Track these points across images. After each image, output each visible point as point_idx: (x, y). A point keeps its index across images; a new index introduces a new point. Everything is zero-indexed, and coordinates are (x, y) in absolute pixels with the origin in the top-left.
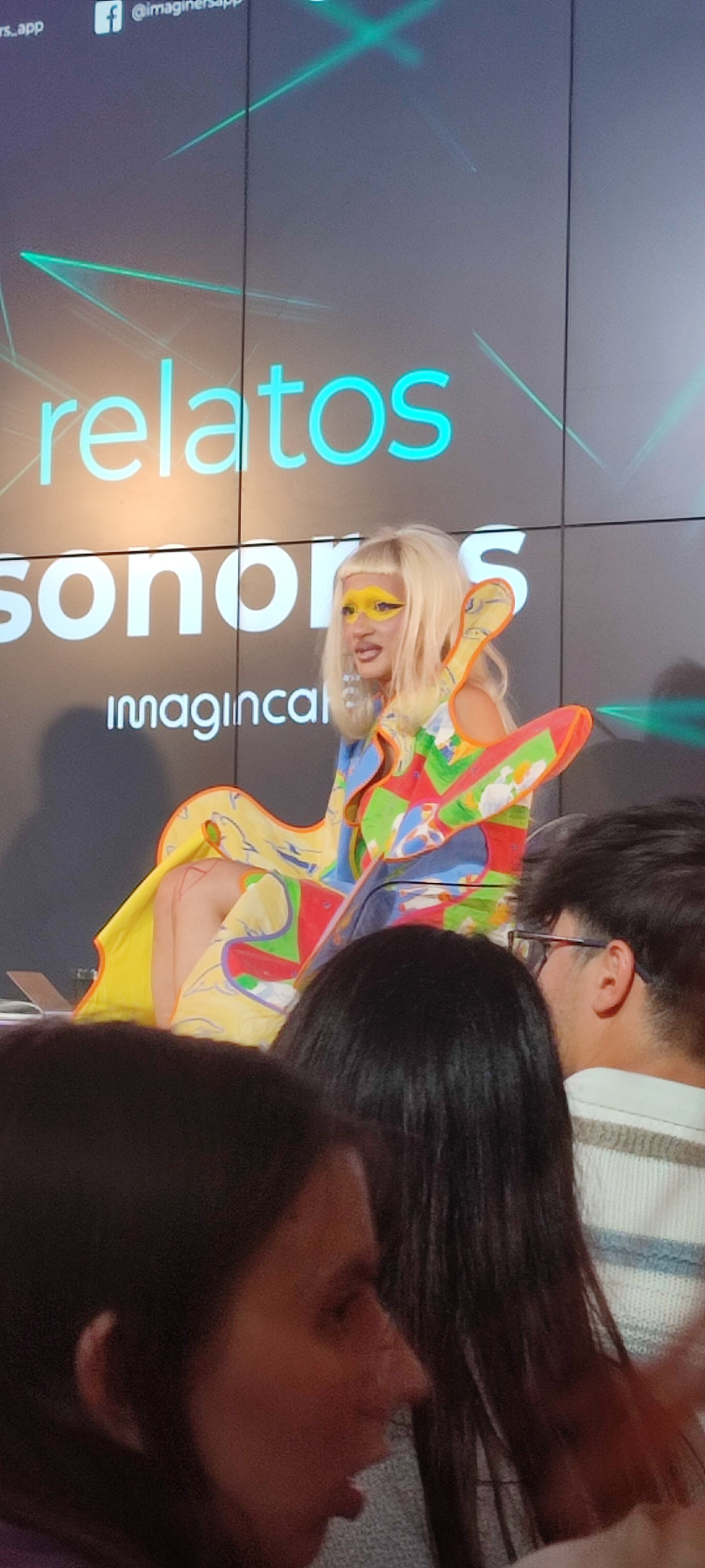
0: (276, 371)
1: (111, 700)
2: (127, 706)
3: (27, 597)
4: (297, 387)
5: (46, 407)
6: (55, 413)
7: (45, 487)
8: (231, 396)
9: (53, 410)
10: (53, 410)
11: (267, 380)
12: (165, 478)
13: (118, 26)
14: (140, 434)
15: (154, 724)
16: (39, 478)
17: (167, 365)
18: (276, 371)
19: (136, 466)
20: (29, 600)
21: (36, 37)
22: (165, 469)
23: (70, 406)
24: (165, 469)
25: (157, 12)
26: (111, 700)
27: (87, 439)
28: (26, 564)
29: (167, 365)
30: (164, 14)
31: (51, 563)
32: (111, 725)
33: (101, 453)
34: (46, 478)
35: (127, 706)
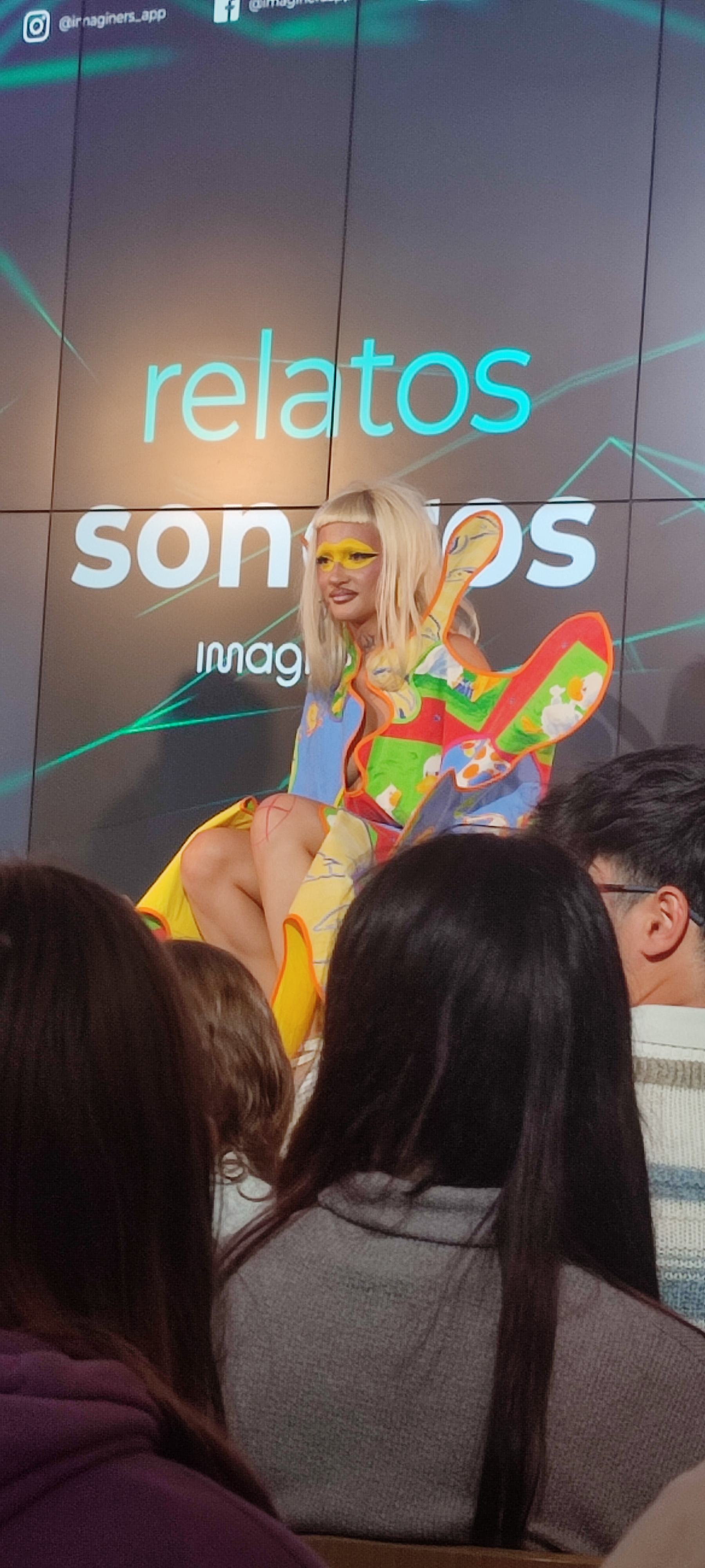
0: (369, 344)
1: (201, 646)
2: (215, 652)
4: (388, 360)
5: (153, 369)
6: (161, 375)
7: (149, 444)
8: (325, 366)
9: (159, 373)
10: (159, 373)
11: (360, 352)
12: (260, 441)
14: (239, 398)
15: (240, 670)
16: (142, 435)
17: (267, 335)
18: (369, 344)
19: (233, 428)
20: (128, 548)
22: (261, 433)
23: (175, 370)
24: (261, 433)
27: (189, 401)
28: (127, 516)
29: (267, 335)
31: (151, 515)
32: (199, 670)
33: (200, 414)
34: (149, 436)
35: (215, 652)
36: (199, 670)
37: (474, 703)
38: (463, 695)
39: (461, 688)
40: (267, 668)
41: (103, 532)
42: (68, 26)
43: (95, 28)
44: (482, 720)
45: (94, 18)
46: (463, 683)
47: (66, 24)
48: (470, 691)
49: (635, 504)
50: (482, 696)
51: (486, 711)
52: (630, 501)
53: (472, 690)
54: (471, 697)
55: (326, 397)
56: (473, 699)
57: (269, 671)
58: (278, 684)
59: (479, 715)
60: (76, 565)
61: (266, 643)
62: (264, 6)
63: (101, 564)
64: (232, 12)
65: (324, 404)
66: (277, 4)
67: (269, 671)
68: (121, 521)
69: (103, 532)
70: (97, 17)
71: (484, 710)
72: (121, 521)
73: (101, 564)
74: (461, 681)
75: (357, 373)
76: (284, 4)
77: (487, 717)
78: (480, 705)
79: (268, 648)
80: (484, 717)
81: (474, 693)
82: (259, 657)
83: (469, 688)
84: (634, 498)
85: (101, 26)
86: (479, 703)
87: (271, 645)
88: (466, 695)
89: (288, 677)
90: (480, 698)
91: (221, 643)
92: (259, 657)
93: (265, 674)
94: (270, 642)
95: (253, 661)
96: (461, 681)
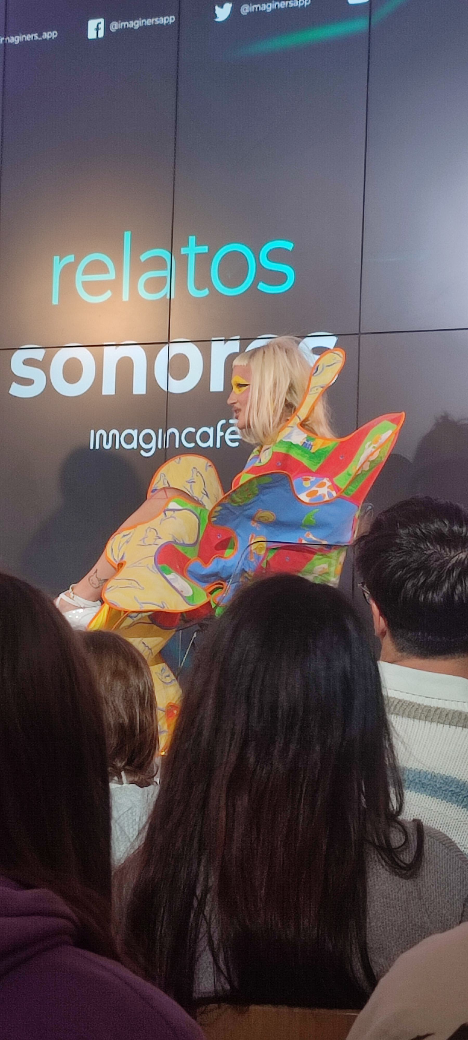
0: (192, 239)
1: (92, 432)
2: (101, 435)
3: (42, 370)
4: (204, 249)
5: (56, 258)
6: (63, 261)
7: (55, 306)
8: (165, 254)
9: (60, 260)
10: (60, 260)
11: (186, 244)
12: (126, 302)
13: (101, 34)
14: (111, 275)
15: (117, 447)
16: (51, 300)
17: (127, 235)
18: (192, 239)
19: (108, 294)
20: (44, 372)
21: (53, 40)
22: (126, 296)
23: (70, 258)
24: (126, 296)
25: (125, 27)
26: (92, 432)
27: (80, 278)
28: (43, 351)
29: (127, 235)
30: (261, 11)
31: (58, 350)
32: (92, 447)
33: (88, 286)
34: (55, 301)
35: (101, 435)
36: (92, 447)
37: (313, 453)
38: (307, 449)
39: (305, 444)
40: (134, 445)
41: (28, 362)
42: (116, 28)
43: (132, 28)
44: (317, 465)
45: (131, 22)
46: (306, 442)
47: (114, 27)
48: (310, 447)
49: (362, 336)
50: (319, 450)
51: (320, 460)
52: (359, 334)
53: (312, 446)
54: (311, 449)
55: (166, 273)
56: (312, 451)
57: (135, 447)
58: (141, 454)
59: (315, 461)
60: (11, 384)
61: (134, 430)
62: (119, 28)
63: (28, 382)
64: (99, 32)
65: (165, 278)
66: (128, 26)
67: (135, 447)
68: (39, 354)
69: (28, 362)
70: (134, 22)
71: (319, 459)
72: (39, 354)
73: (28, 382)
74: (305, 441)
75: (186, 256)
76: (132, 26)
77: (321, 464)
78: (314, 456)
79: (135, 433)
80: (319, 463)
81: (313, 447)
82: (129, 438)
83: (310, 445)
84: (362, 332)
85: (17, 42)
86: (316, 454)
87: (136, 431)
88: (308, 448)
89: (148, 451)
90: (316, 451)
91: (104, 429)
92: (129, 438)
93: (133, 448)
94: (136, 428)
95: (125, 442)
96: (305, 441)
